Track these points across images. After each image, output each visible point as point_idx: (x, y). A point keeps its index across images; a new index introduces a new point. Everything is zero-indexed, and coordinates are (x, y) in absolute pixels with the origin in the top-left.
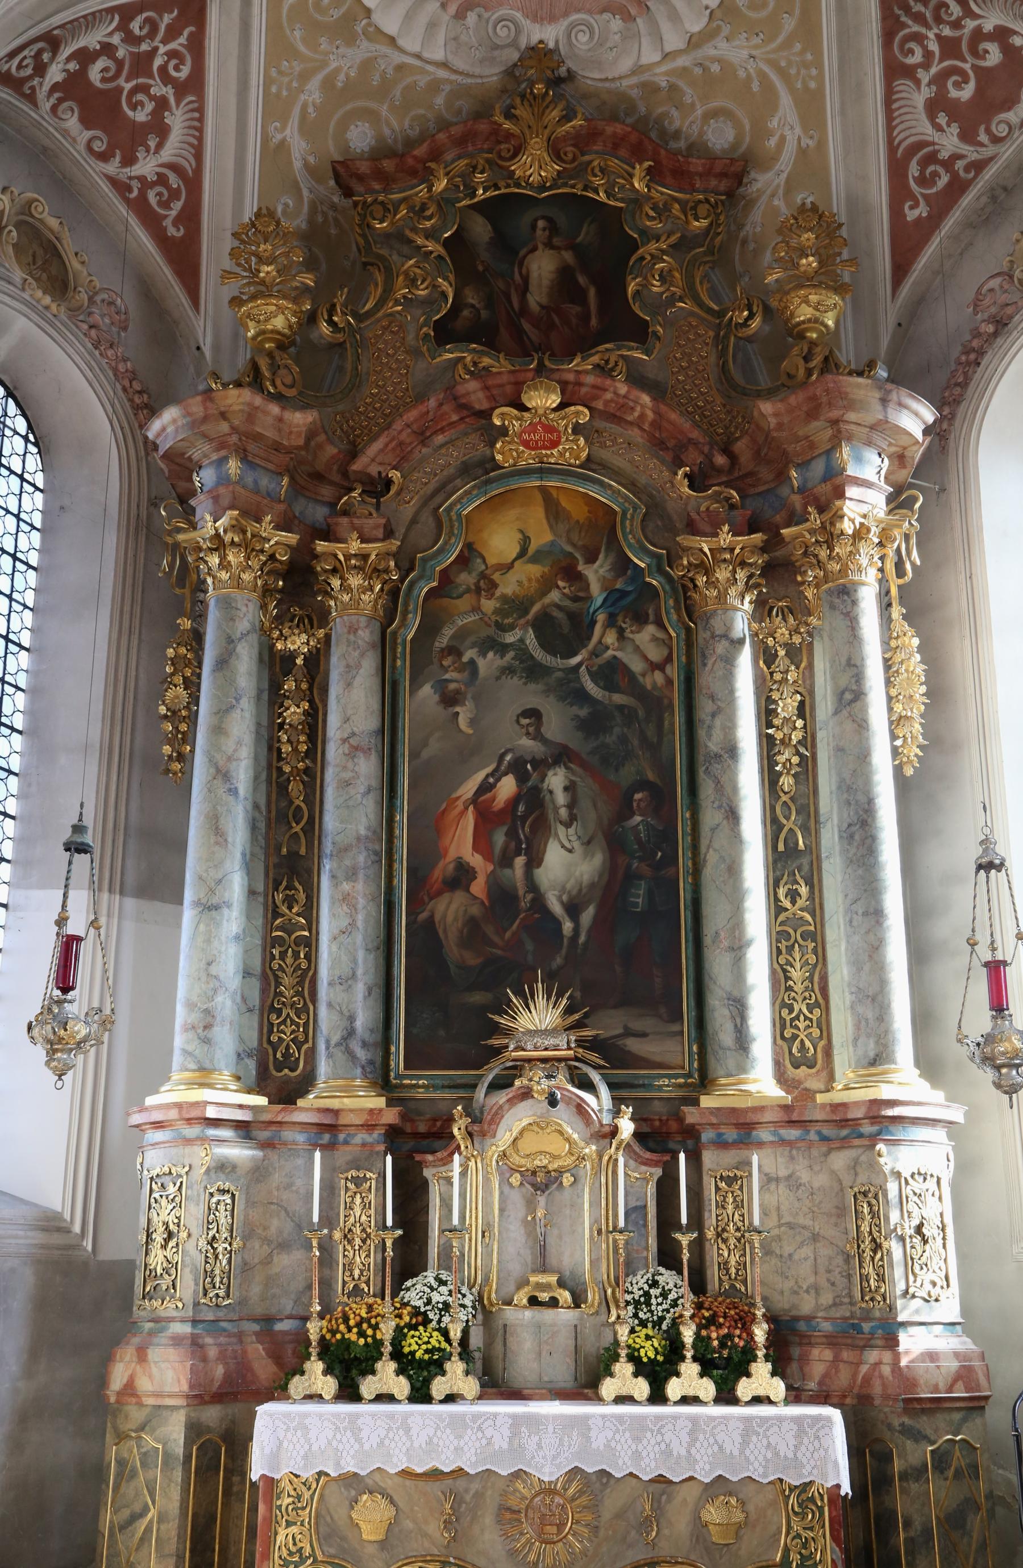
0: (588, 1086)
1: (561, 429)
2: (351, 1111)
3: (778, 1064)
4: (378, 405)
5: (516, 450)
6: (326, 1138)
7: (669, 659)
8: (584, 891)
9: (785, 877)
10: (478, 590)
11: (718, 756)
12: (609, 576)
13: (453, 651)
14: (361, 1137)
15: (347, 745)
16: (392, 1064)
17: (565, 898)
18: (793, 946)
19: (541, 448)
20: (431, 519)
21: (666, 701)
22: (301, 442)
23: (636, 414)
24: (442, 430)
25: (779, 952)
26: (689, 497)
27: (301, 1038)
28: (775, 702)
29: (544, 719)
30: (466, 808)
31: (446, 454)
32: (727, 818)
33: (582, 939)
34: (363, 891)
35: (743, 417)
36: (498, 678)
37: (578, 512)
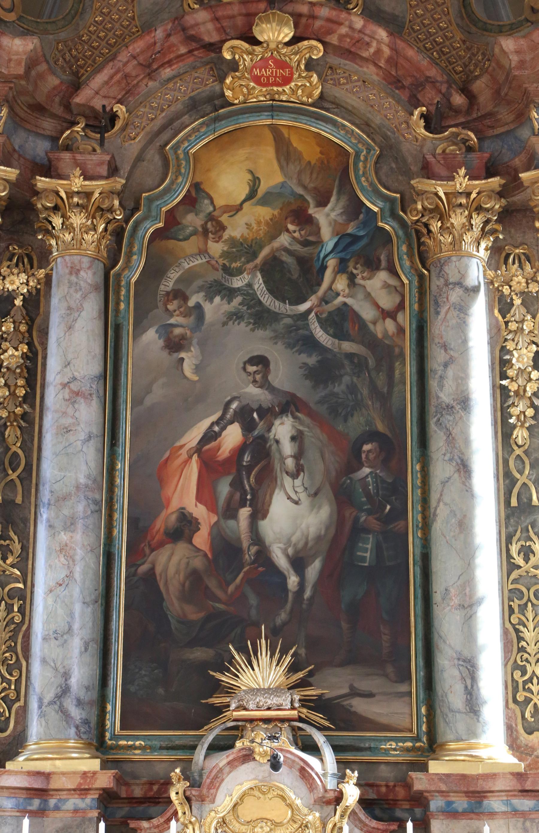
0: (312, 748)
1: (294, 65)
2: (63, 774)
3: (510, 729)
4: (102, 34)
5: (247, 87)
6: (36, 803)
7: (401, 306)
8: (310, 544)
9: (518, 534)
10: (205, 232)
11: (450, 408)
12: (340, 220)
13: (179, 294)
14: (73, 802)
15: (67, 390)
16: (108, 723)
17: (290, 551)
18: (526, 605)
19: (273, 85)
20: (157, 158)
21: (397, 350)
22: (21, 71)
23: (372, 50)
24: (169, 63)
25: (511, 611)
26: (424, 139)
27: (12, 695)
28: (510, 352)
29: (272, 366)
30: (190, 457)
31: (172, 89)
32: (459, 471)
33: (308, 594)
34: (82, 543)
35: (484, 54)
36: (225, 324)
37: (310, 152)
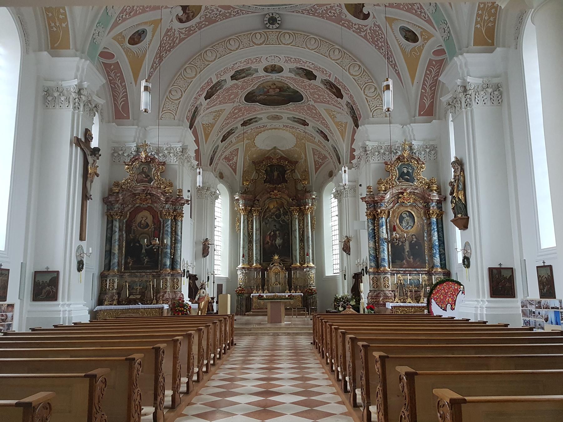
13: (266, 218)
